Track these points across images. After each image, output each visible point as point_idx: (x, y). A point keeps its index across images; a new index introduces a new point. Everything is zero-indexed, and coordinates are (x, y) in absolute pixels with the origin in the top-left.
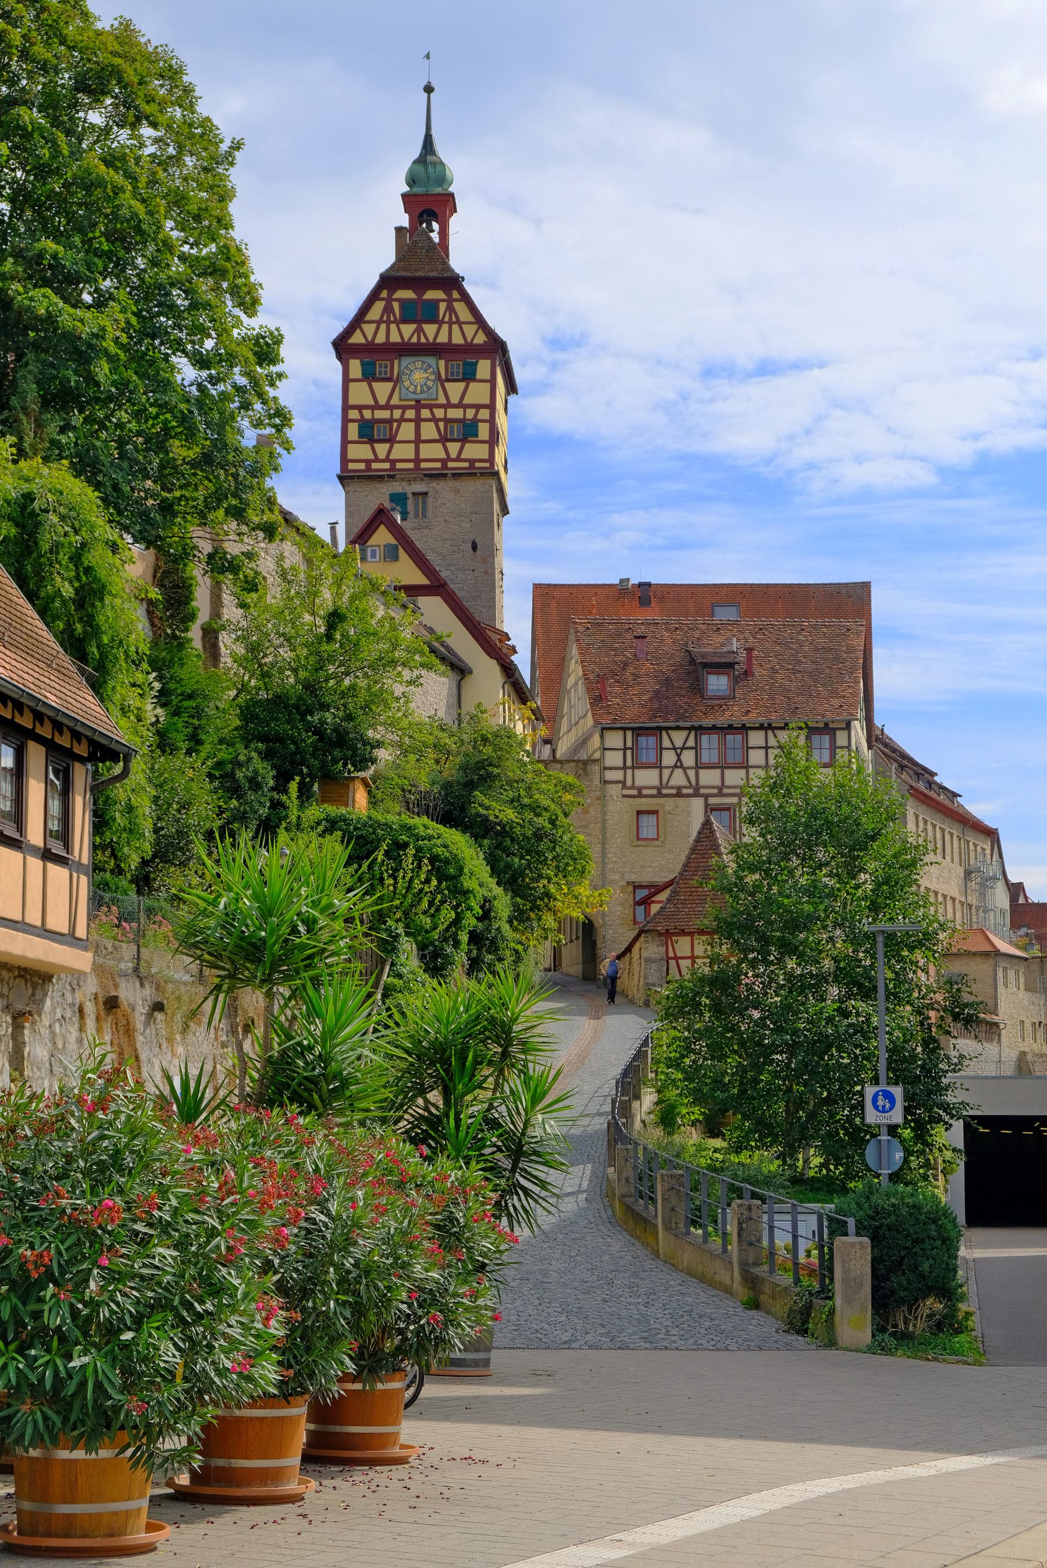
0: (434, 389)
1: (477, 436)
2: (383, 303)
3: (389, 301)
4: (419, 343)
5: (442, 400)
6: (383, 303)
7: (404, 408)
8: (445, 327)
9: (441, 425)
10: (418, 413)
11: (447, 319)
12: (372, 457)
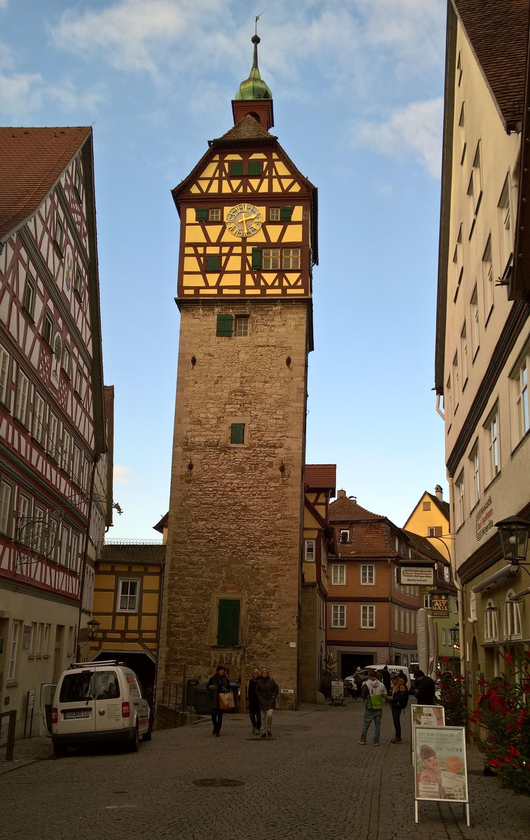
2: (217, 164)
6: (217, 164)
8: (266, 181)
12: (203, 284)
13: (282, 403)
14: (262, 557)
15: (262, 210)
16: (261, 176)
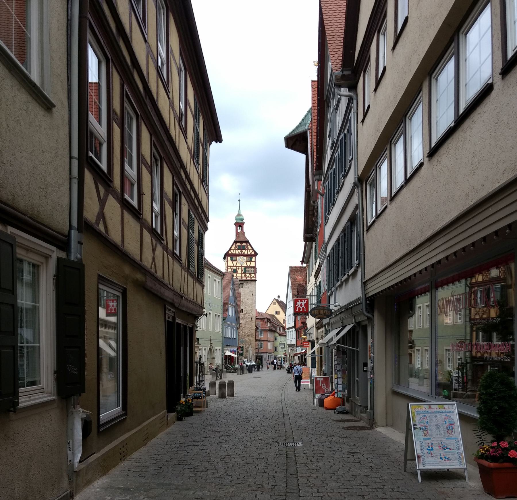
3: (236, 245)
13: (251, 304)
14: (248, 337)
15: (245, 258)
16: (245, 249)
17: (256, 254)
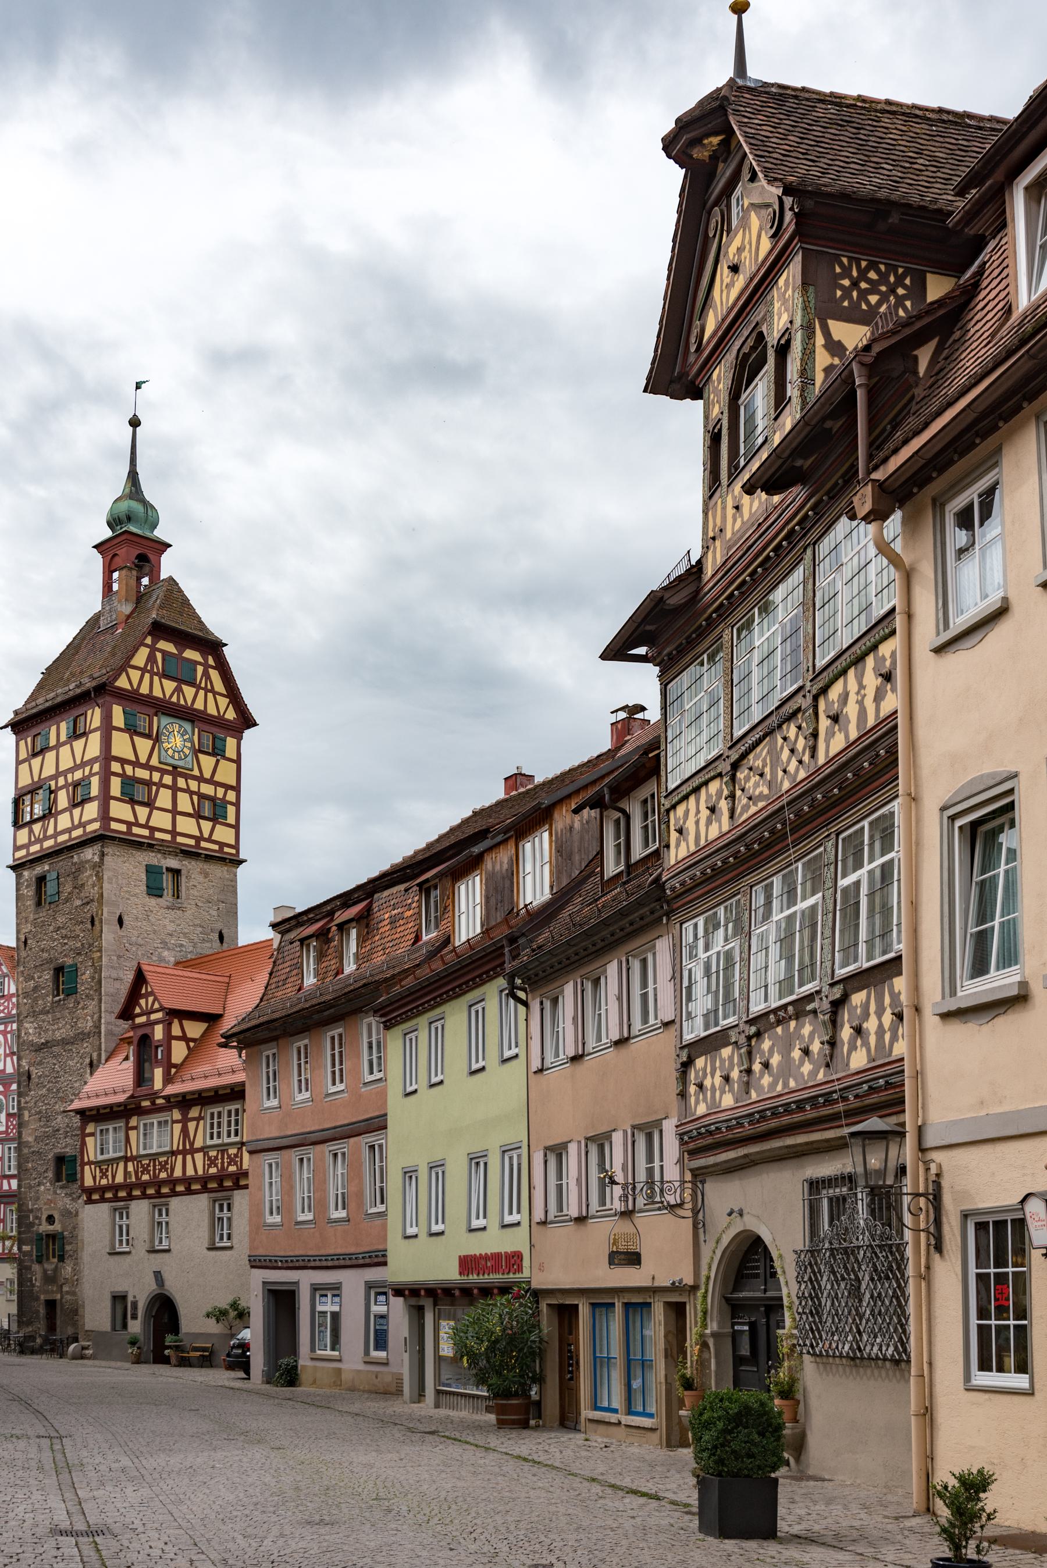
0: (189, 758)
1: (225, 818)
3: (153, 649)
4: (178, 704)
5: (196, 772)
7: (163, 772)
9: (195, 798)
10: (175, 781)
11: (203, 685)
16: (192, 684)
17: (246, 721)
